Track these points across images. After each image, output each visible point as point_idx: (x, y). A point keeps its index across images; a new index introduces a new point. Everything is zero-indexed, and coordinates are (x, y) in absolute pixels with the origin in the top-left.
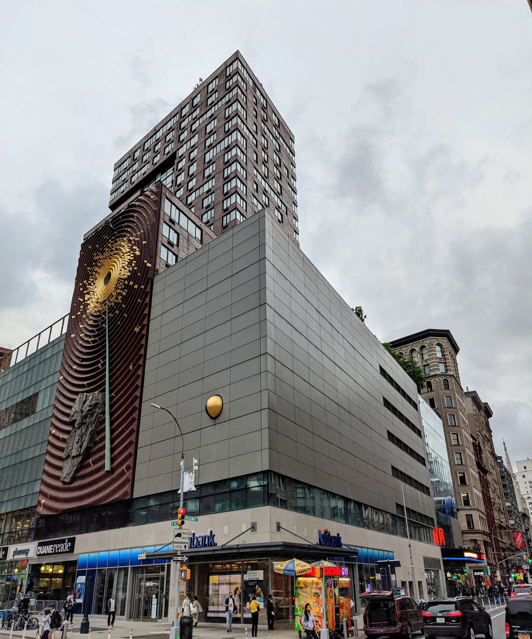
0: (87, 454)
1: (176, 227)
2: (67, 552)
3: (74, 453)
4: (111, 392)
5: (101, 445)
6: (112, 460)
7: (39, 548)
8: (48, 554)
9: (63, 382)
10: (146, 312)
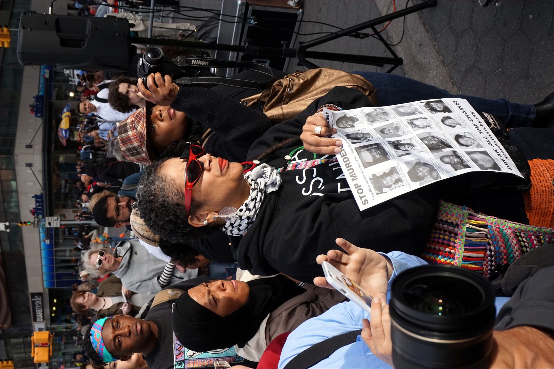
2: (42, 298)
7: (38, 320)
8: (43, 312)
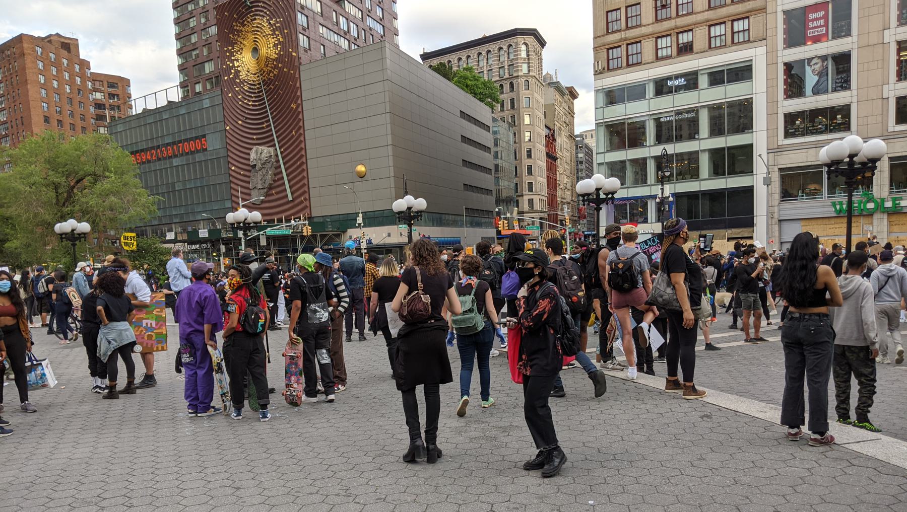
0: (270, 188)
1: (306, 12)
3: (260, 186)
4: (280, 148)
5: (280, 182)
6: (292, 193)
9: (231, 132)
10: (299, 94)
